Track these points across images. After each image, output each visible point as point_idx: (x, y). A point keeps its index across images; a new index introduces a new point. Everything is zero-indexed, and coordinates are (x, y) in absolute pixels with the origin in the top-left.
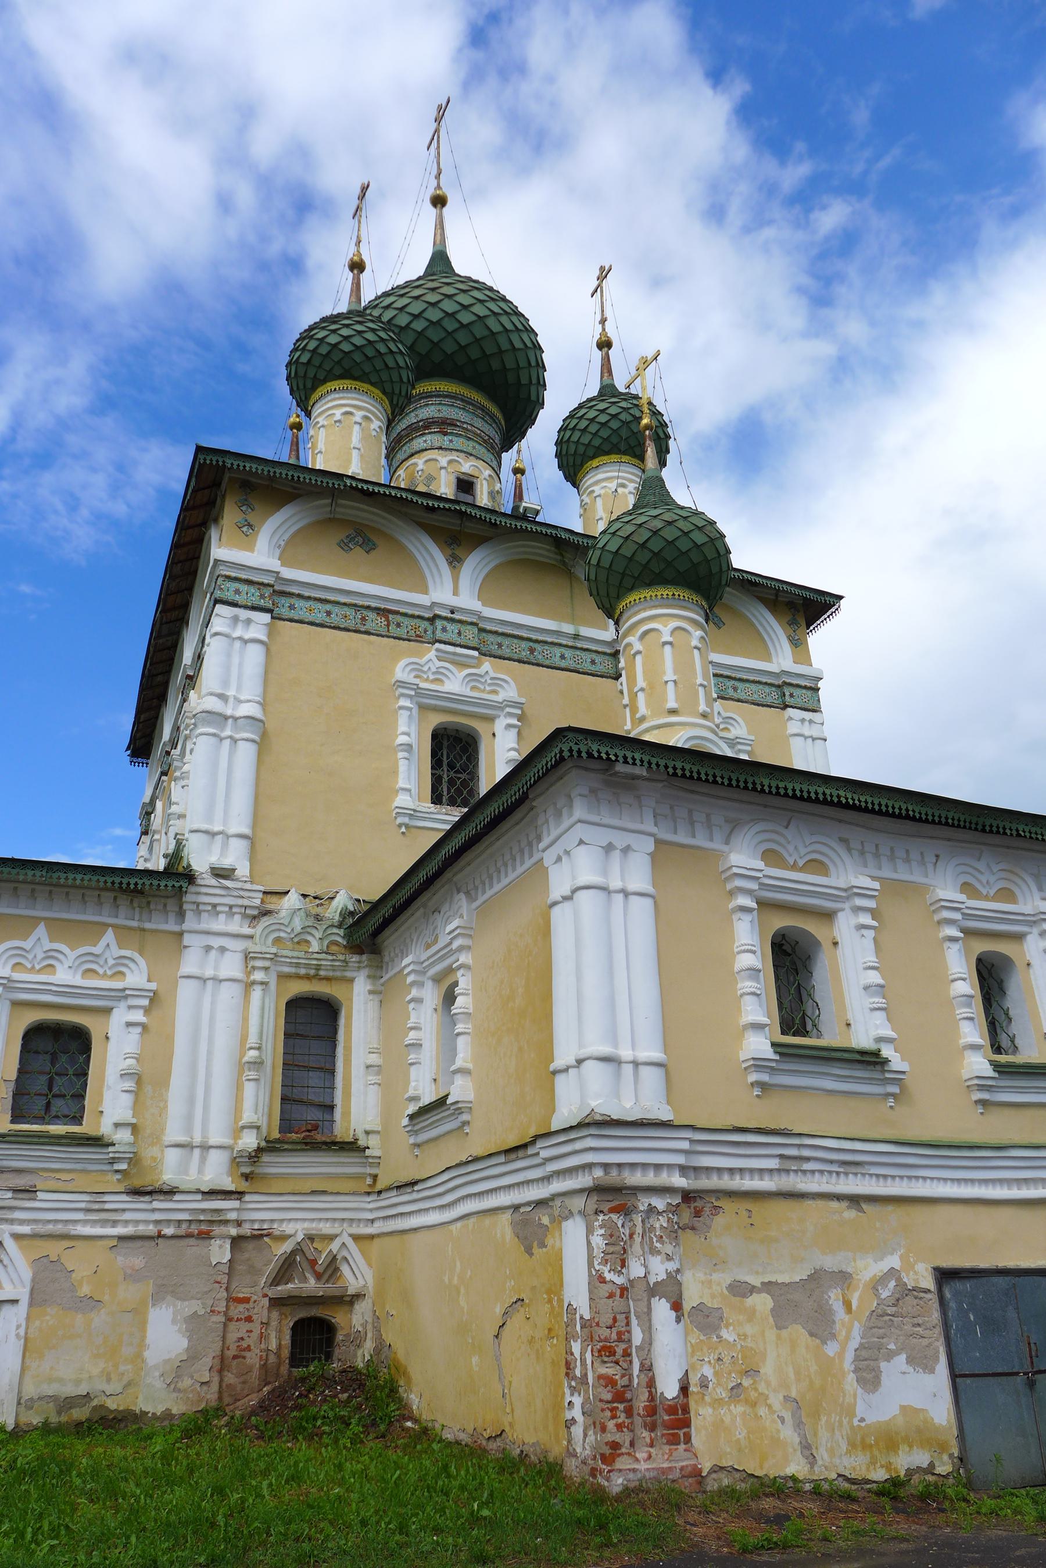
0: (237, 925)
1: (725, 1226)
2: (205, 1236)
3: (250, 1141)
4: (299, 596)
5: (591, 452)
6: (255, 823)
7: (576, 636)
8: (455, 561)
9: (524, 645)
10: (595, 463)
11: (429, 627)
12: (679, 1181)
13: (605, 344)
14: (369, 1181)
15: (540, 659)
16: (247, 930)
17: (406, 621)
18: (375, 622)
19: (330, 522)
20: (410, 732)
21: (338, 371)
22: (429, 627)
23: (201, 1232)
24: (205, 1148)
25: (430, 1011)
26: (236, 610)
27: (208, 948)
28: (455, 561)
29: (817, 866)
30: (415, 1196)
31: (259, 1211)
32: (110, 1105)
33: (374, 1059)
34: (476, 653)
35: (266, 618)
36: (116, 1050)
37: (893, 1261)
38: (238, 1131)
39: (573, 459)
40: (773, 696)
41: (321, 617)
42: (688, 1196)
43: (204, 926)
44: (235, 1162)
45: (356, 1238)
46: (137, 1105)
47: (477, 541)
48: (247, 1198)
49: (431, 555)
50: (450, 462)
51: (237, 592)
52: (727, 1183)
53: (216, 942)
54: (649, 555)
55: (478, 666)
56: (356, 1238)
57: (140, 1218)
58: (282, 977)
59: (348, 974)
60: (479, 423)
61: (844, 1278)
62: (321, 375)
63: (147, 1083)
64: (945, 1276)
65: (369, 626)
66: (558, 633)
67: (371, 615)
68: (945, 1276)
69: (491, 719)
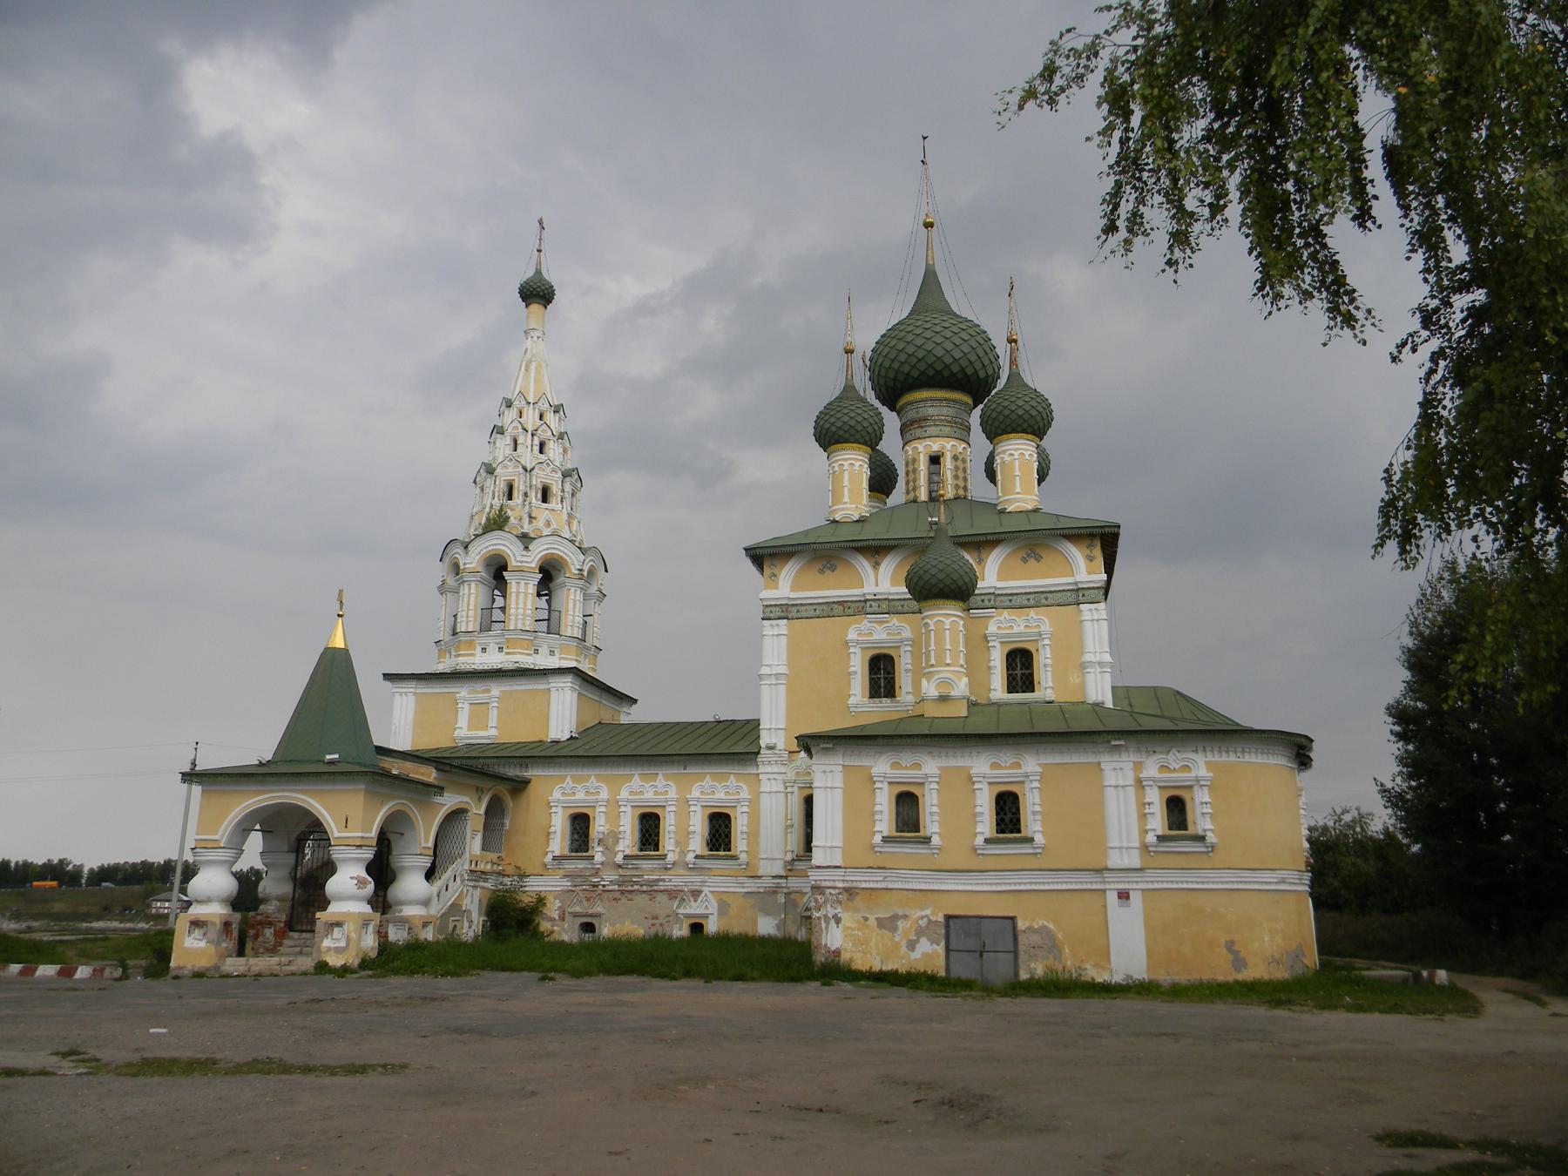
1: (858, 902)
2: (775, 892)
3: (789, 857)
8: (876, 565)
11: (860, 608)
12: (840, 885)
20: (858, 665)
22: (860, 608)
23: (774, 891)
28: (876, 565)
29: (918, 766)
32: (739, 844)
36: (740, 825)
37: (928, 912)
40: (1072, 597)
41: (812, 613)
42: (847, 890)
46: (749, 844)
49: (863, 564)
52: (864, 885)
57: (751, 886)
60: (945, 411)
61: (905, 917)
63: (753, 835)
64: (948, 918)
65: (835, 612)
68: (948, 918)
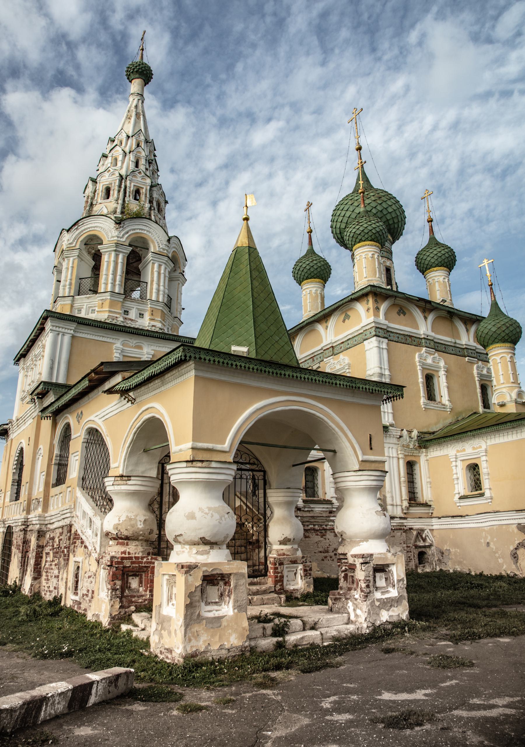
0: (395, 441)
4: (391, 332)
5: (434, 265)
6: (393, 410)
7: (455, 343)
9: (443, 346)
10: (435, 269)
13: (430, 221)
14: (430, 514)
15: (447, 351)
16: (397, 443)
17: (416, 340)
18: (409, 340)
19: (394, 305)
21: (369, 239)
24: (397, 505)
25: (460, 470)
26: (380, 338)
27: (389, 448)
30: (463, 519)
31: (410, 523)
33: (428, 480)
34: (434, 350)
35: (386, 341)
38: (402, 500)
39: (423, 266)
41: (396, 339)
43: (388, 441)
44: (402, 510)
45: (430, 530)
47: (431, 311)
48: (408, 519)
50: (383, 261)
51: (379, 332)
53: (391, 446)
54: (505, 334)
55: (434, 354)
56: (430, 530)
58: (405, 456)
59: (420, 455)
62: (363, 239)
66: (451, 342)
67: (408, 338)
69: (438, 371)
